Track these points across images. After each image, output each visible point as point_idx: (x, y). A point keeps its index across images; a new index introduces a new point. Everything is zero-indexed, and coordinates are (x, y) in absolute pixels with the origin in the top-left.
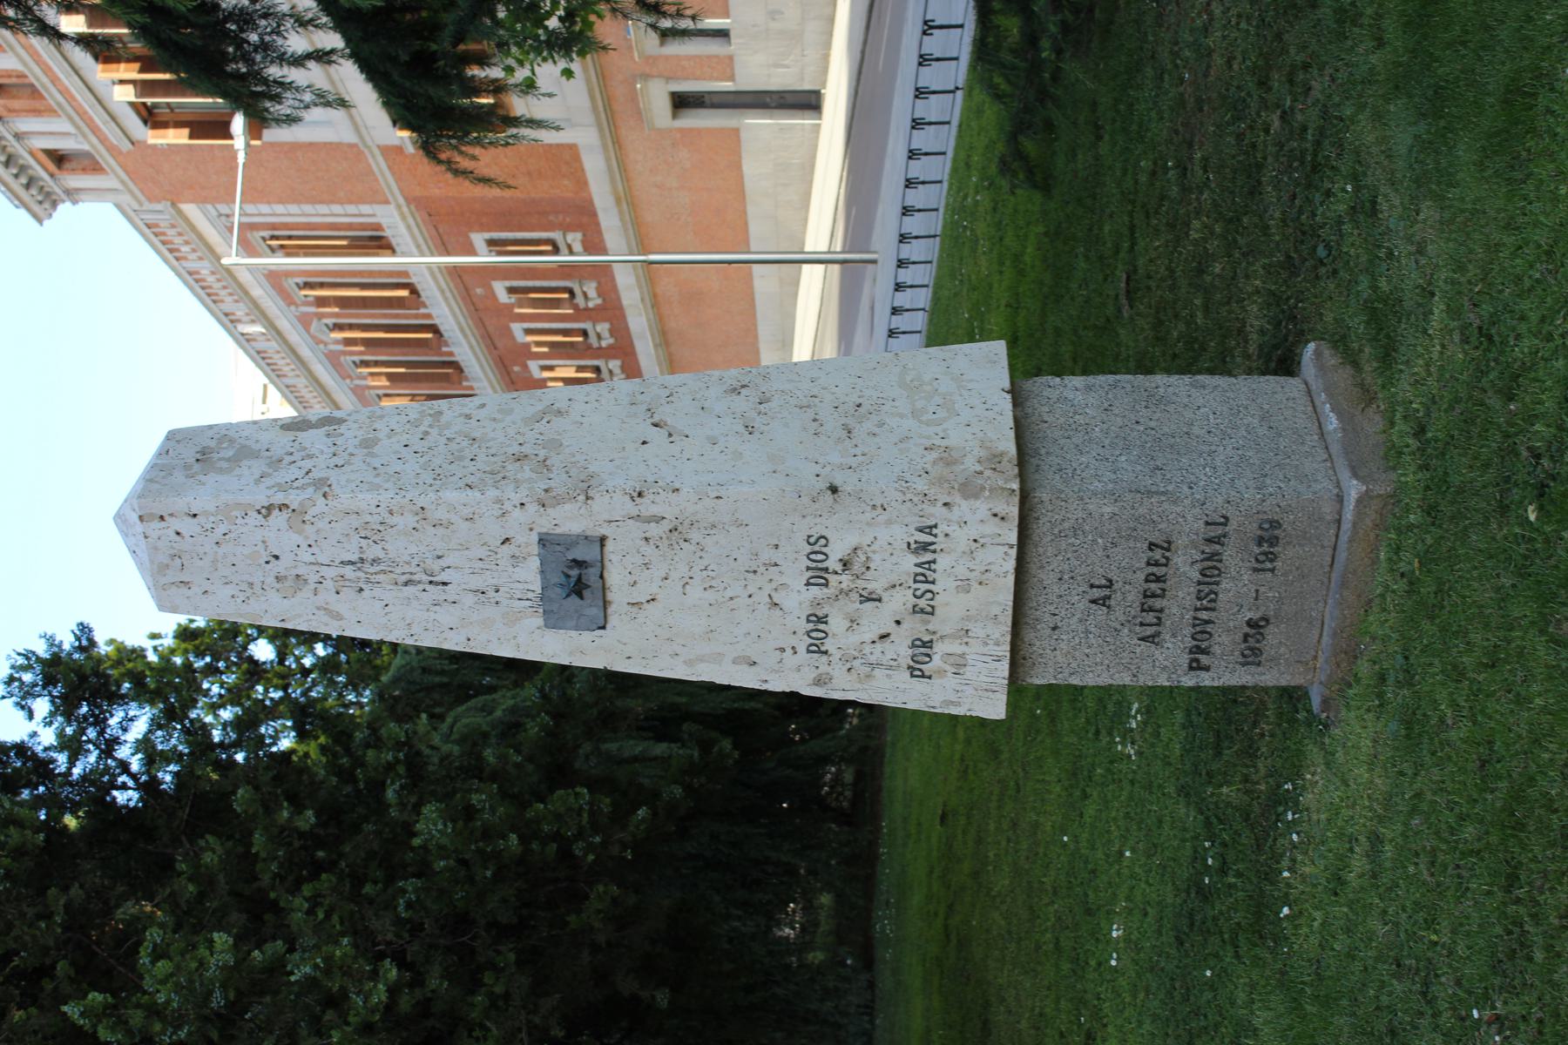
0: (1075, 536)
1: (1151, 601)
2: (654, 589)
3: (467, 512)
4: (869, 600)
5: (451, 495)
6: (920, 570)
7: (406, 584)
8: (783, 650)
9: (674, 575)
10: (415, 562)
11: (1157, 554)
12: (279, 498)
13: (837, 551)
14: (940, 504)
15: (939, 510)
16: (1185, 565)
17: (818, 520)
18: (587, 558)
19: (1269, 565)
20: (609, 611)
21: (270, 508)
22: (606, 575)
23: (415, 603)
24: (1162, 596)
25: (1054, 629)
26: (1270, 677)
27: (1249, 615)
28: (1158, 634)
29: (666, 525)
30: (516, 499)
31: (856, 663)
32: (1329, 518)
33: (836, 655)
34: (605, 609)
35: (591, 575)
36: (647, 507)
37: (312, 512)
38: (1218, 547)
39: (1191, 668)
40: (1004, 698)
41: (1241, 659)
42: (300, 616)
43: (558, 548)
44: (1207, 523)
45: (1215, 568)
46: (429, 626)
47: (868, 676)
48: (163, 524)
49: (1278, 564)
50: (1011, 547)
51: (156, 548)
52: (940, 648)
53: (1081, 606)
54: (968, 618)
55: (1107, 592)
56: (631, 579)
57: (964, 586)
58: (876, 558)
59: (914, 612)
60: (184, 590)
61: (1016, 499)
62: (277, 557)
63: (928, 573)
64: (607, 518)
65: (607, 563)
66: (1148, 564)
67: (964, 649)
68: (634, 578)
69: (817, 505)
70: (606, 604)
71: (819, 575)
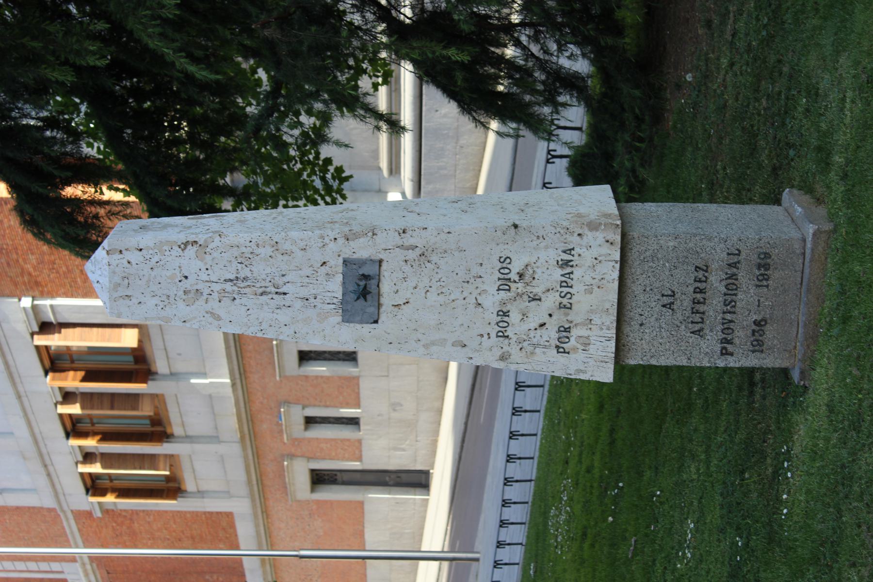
0: (653, 261)
1: (697, 307)
2: (409, 295)
3: (302, 244)
4: (534, 299)
5: (294, 234)
6: (563, 279)
7: (262, 294)
8: (482, 336)
9: (421, 285)
10: (268, 279)
11: (700, 274)
12: (191, 238)
13: (516, 267)
14: (576, 234)
15: (576, 238)
16: (716, 281)
17: (506, 246)
18: (371, 273)
19: (765, 283)
20: (382, 310)
21: (186, 244)
22: (381, 285)
23: (266, 307)
24: (704, 303)
25: (641, 325)
26: (770, 361)
27: (755, 317)
28: (701, 330)
29: (418, 252)
30: (332, 235)
31: (525, 344)
32: (798, 252)
34: (379, 309)
36: (409, 241)
37: (211, 246)
38: (735, 270)
39: (722, 354)
40: (612, 366)
42: (195, 318)
43: (355, 267)
44: (728, 254)
45: (733, 284)
46: (273, 323)
47: (532, 353)
48: (121, 256)
49: (770, 282)
50: (616, 262)
51: (114, 272)
52: (575, 333)
53: (657, 309)
55: (671, 300)
56: (395, 288)
58: (539, 271)
59: (560, 307)
60: (127, 301)
61: (620, 230)
62: (186, 277)
63: (568, 280)
64: (384, 247)
65: (382, 278)
66: (695, 281)
67: (588, 333)
69: (506, 237)
70: (379, 306)
71: (505, 283)
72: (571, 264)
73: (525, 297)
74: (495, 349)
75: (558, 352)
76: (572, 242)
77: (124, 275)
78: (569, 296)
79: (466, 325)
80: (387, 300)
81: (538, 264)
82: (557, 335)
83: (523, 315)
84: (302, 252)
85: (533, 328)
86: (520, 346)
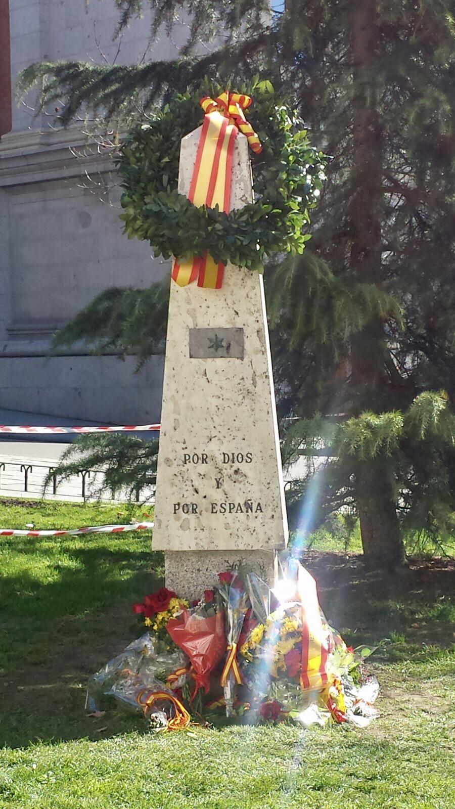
2: (214, 382)
3: (252, 295)
4: (218, 483)
6: (236, 506)
8: (184, 443)
13: (244, 467)
15: (270, 513)
29: (251, 388)
31: (180, 478)
33: (184, 469)
35: (221, 351)
52: (192, 516)
56: (220, 371)
58: (241, 486)
59: (212, 504)
63: (235, 509)
69: (268, 458)
71: (229, 459)
72: (249, 510)
73: (219, 476)
74: (174, 454)
75: (175, 505)
79: (192, 429)
81: (247, 484)
82: (189, 503)
83: (204, 475)
84: (246, 295)
85: (193, 483)
86: (178, 474)
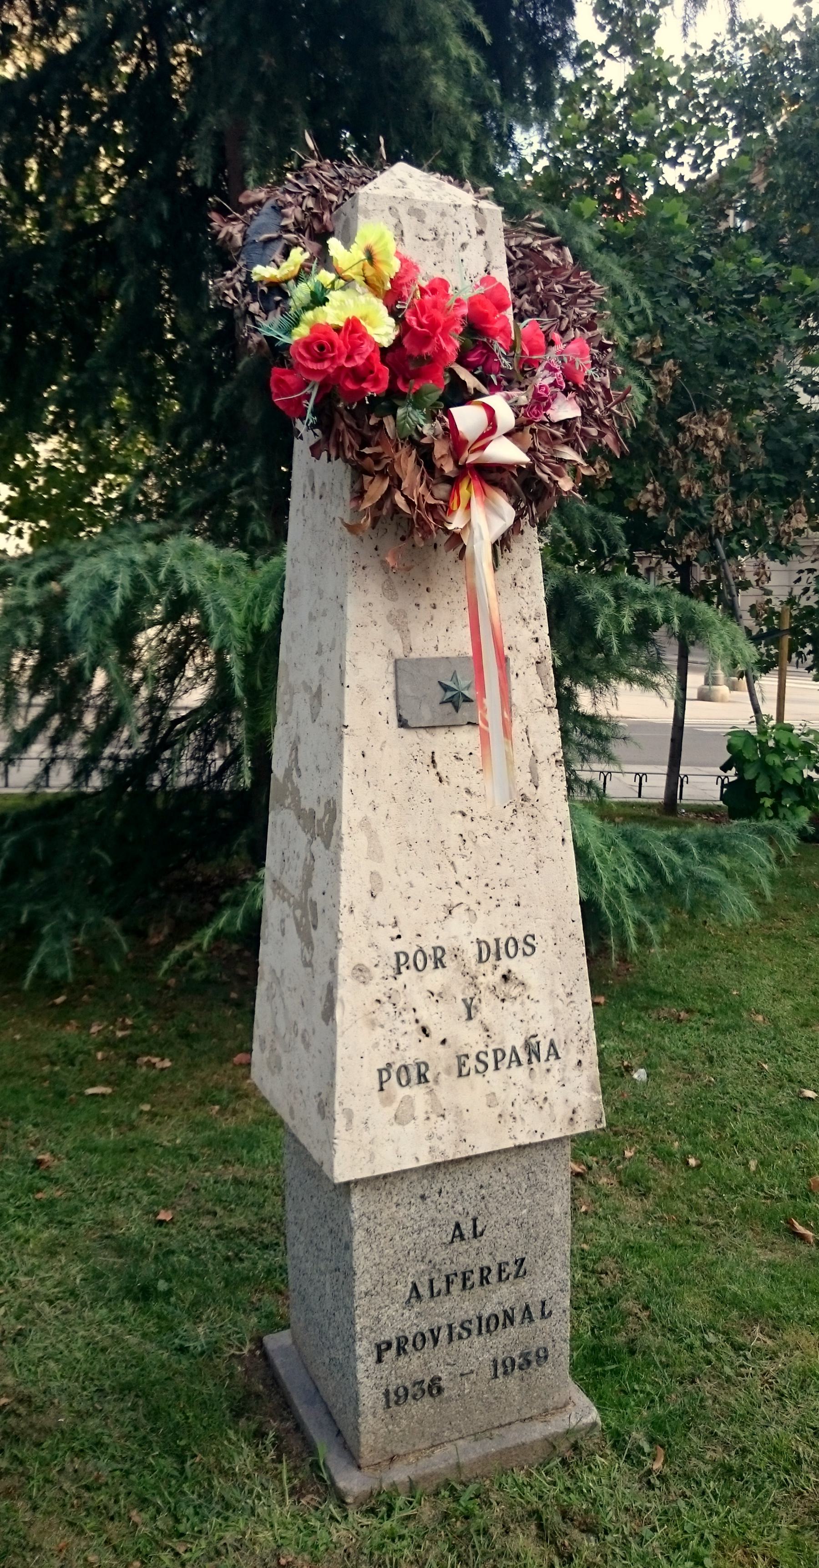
1: (458, 1280)
2: (454, 781)
6: (508, 1052)
9: (473, 801)
13: (519, 966)
14: (580, 1057)
15: (574, 1058)
17: (551, 943)
19: (500, 1370)
20: (422, 732)
27: (444, 1376)
29: (529, 790)
31: (388, 1007)
41: (392, 1388)
49: (501, 1378)
51: (443, 214)
52: (417, 1092)
54: (459, 1113)
56: (464, 755)
57: (492, 1100)
58: (516, 1007)
64: (532, 729)
68: (465, 757)
71: (489, 951)
72: (534, 1059)
73: (470, 992)
75: (380, 1071)
76: (568, 1052)
77: (441, 232)
78: (481, 1067)
79: (411, 892)
80: (442, 742)
81: (527, 1001)
82: (409, 1062)
83: (440, 995)
84: (511, 581)
85: (418, 1015)
86: (384, 999)
